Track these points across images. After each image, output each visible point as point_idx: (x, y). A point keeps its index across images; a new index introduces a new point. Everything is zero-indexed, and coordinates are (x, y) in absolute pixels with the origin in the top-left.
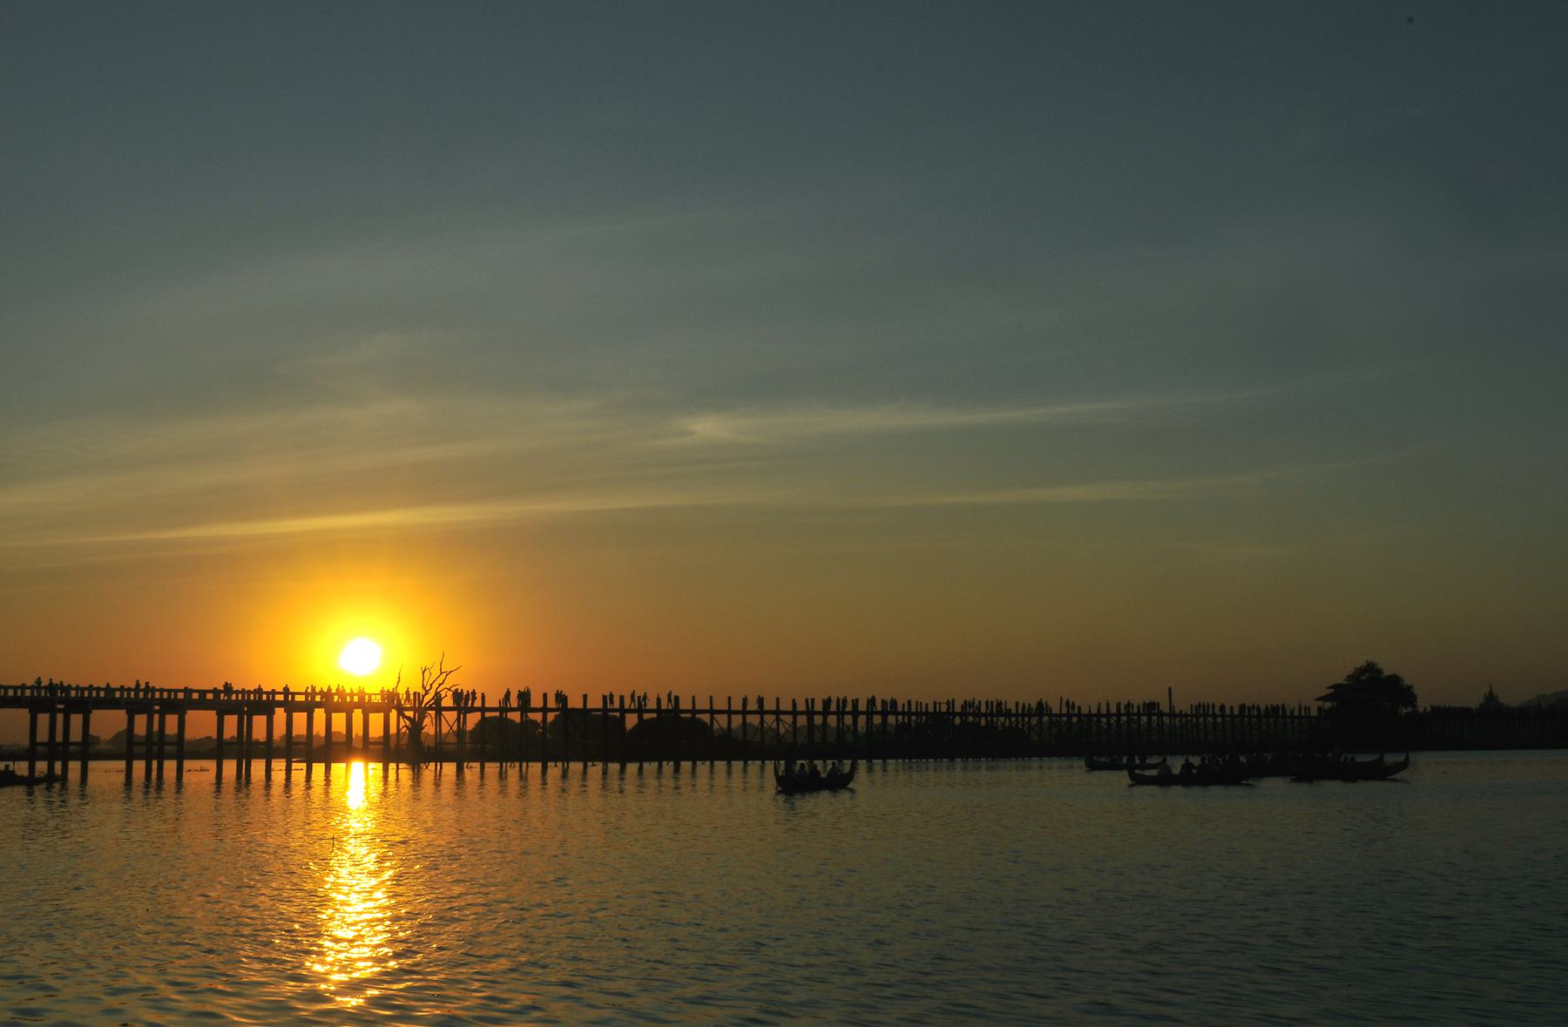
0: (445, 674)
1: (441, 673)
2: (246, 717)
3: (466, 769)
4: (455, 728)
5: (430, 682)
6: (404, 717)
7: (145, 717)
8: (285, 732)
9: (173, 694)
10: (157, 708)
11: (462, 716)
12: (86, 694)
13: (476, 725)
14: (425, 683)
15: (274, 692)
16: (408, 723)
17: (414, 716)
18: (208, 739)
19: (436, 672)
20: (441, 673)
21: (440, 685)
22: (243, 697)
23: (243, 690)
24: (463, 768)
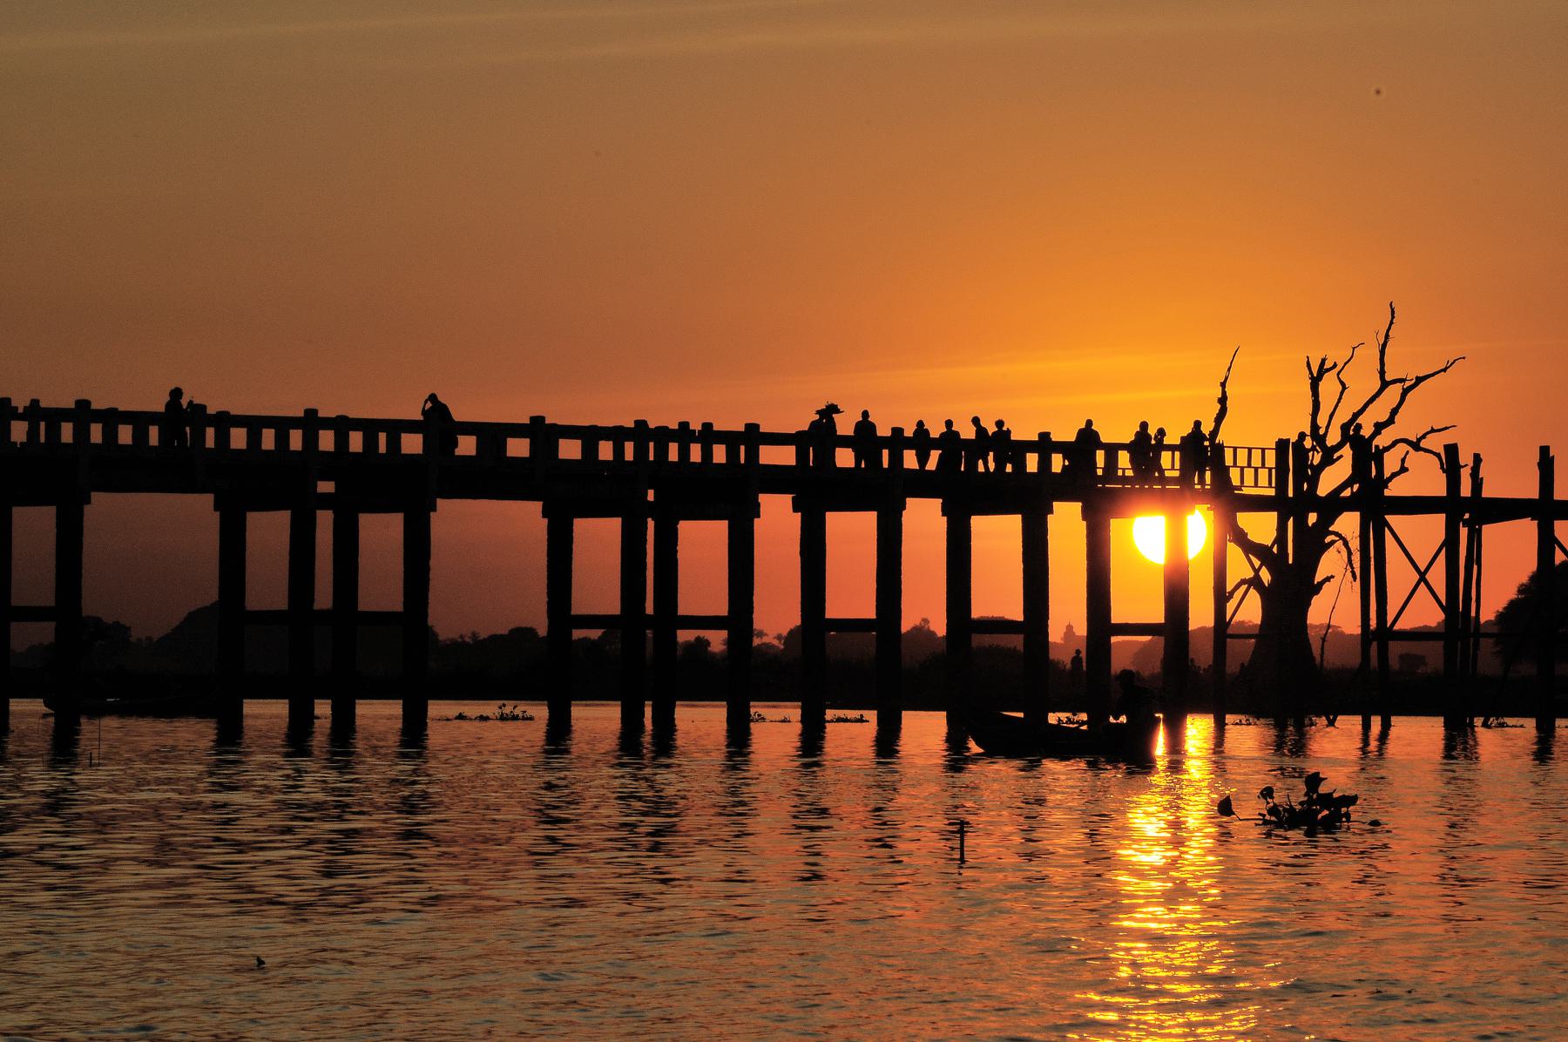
0: (1398, 388)
1: (1385, 384)
2: (651, 523)
4: (1438, 576)
6: (1241, 538)
7: (283, 518)
8: (796, 620)
9: (382, 437)
10: (326, 487)
12: (67, 432)
13: (1522, 589)
14: (1322, 421)
15: (753, 436)
17: (1281, 538)
18: (522, 635)
19: (1362, 382)
20: (1385, 384)
22: (641, 451)
23: (641, 424)
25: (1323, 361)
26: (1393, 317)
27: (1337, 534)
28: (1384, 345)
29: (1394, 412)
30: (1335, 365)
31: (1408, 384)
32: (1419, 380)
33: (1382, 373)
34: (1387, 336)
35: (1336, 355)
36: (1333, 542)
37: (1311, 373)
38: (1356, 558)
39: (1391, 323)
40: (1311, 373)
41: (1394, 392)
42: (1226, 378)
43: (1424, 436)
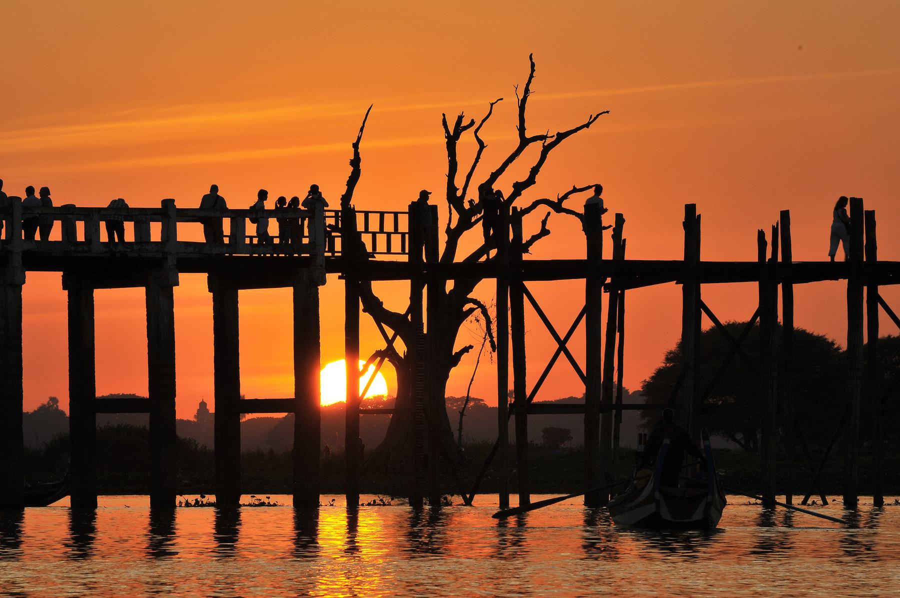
1: (525, 142)
14: (459, 182)
20: (525, 142)
25: (460, 118)
26: (533, 70)
27: (475, 302)
28: (524, 100)
29: (535, 171)
30: (472, 123)
31: (549, 141)
32: (561, 137)
33: (522, 129)
34: (527, 91)
35: (474, 110)
37: (447, 131)
39: (531, 76)
40: (447, 131)
41: (535, 149)
43: (565, 197)
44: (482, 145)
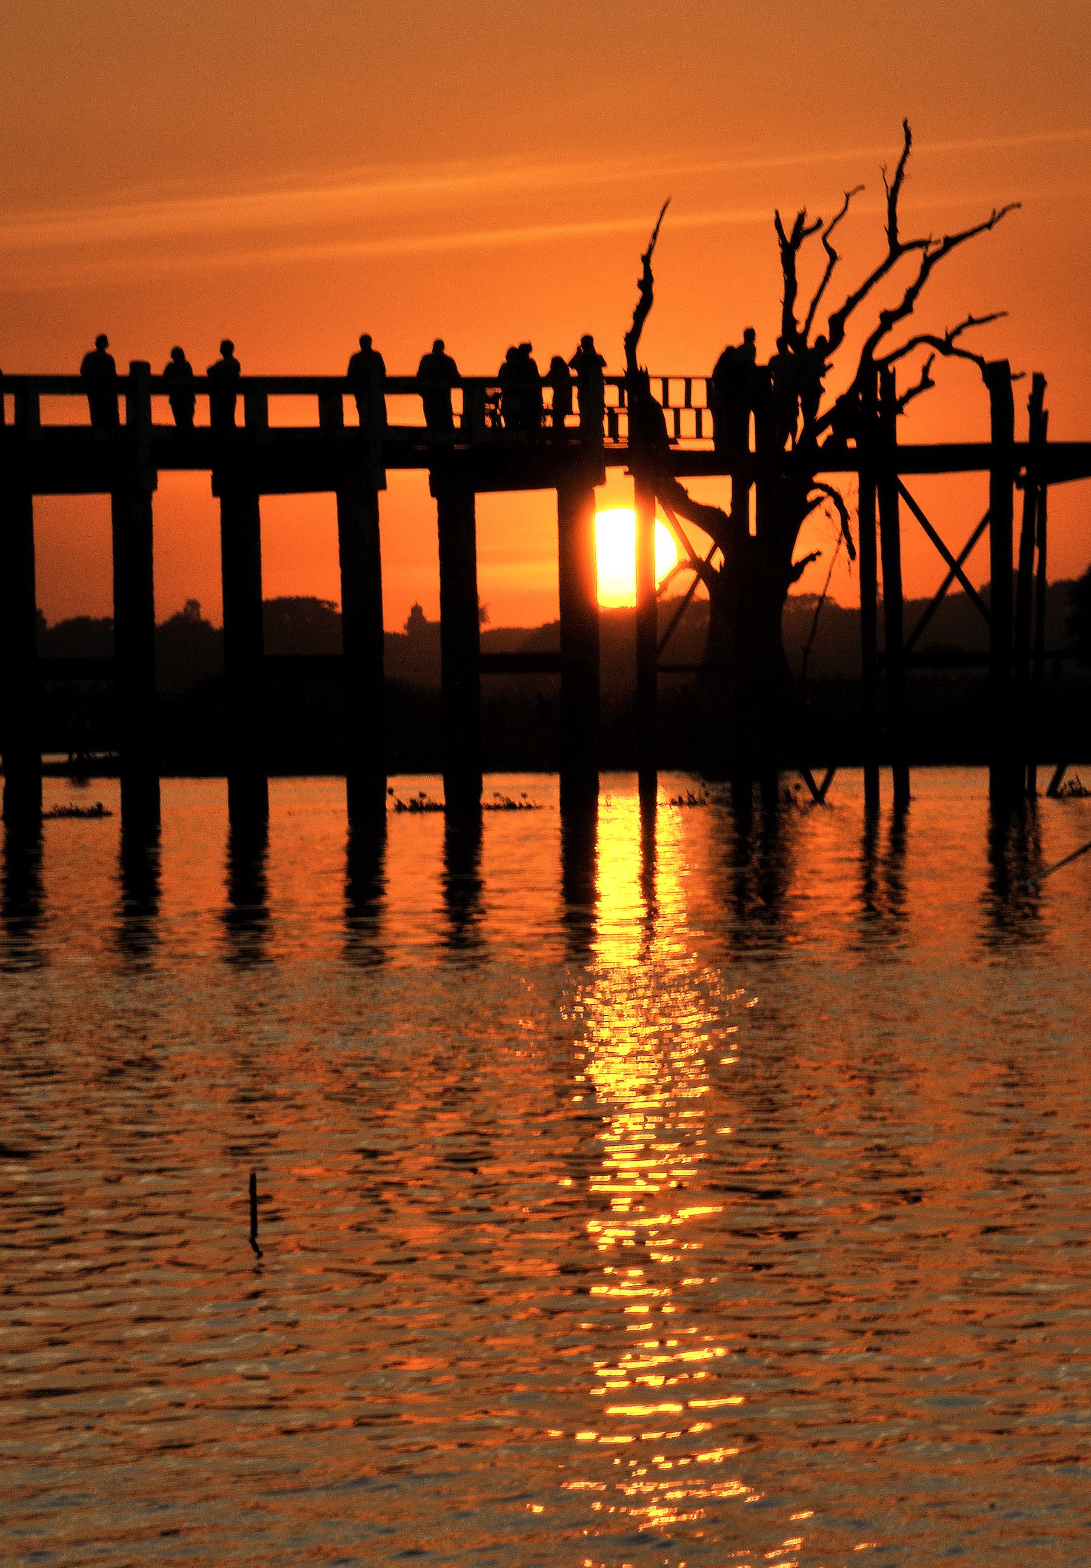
1: (896, 250)
3: (1046, 804)
5: (831, 303)
11: (1018, 497)
14: (800, 311)
16: (703, 542)
20: (896, 250)
21: (888, 319)
24: (1033, 795)
25: (801, 217)
29: (912, 294)
30: (820, 223)
31: (932, 249)
32: (950, 243)
33: (892, 232)
34: (900, 174)
36: (819, 501)
38: (854, 525)
39: (906, 152)
41: (912, 261)
42: (651, 248)
43: (958, 331)
44: (833, 256)
